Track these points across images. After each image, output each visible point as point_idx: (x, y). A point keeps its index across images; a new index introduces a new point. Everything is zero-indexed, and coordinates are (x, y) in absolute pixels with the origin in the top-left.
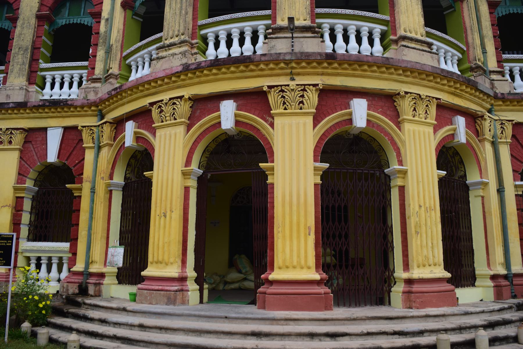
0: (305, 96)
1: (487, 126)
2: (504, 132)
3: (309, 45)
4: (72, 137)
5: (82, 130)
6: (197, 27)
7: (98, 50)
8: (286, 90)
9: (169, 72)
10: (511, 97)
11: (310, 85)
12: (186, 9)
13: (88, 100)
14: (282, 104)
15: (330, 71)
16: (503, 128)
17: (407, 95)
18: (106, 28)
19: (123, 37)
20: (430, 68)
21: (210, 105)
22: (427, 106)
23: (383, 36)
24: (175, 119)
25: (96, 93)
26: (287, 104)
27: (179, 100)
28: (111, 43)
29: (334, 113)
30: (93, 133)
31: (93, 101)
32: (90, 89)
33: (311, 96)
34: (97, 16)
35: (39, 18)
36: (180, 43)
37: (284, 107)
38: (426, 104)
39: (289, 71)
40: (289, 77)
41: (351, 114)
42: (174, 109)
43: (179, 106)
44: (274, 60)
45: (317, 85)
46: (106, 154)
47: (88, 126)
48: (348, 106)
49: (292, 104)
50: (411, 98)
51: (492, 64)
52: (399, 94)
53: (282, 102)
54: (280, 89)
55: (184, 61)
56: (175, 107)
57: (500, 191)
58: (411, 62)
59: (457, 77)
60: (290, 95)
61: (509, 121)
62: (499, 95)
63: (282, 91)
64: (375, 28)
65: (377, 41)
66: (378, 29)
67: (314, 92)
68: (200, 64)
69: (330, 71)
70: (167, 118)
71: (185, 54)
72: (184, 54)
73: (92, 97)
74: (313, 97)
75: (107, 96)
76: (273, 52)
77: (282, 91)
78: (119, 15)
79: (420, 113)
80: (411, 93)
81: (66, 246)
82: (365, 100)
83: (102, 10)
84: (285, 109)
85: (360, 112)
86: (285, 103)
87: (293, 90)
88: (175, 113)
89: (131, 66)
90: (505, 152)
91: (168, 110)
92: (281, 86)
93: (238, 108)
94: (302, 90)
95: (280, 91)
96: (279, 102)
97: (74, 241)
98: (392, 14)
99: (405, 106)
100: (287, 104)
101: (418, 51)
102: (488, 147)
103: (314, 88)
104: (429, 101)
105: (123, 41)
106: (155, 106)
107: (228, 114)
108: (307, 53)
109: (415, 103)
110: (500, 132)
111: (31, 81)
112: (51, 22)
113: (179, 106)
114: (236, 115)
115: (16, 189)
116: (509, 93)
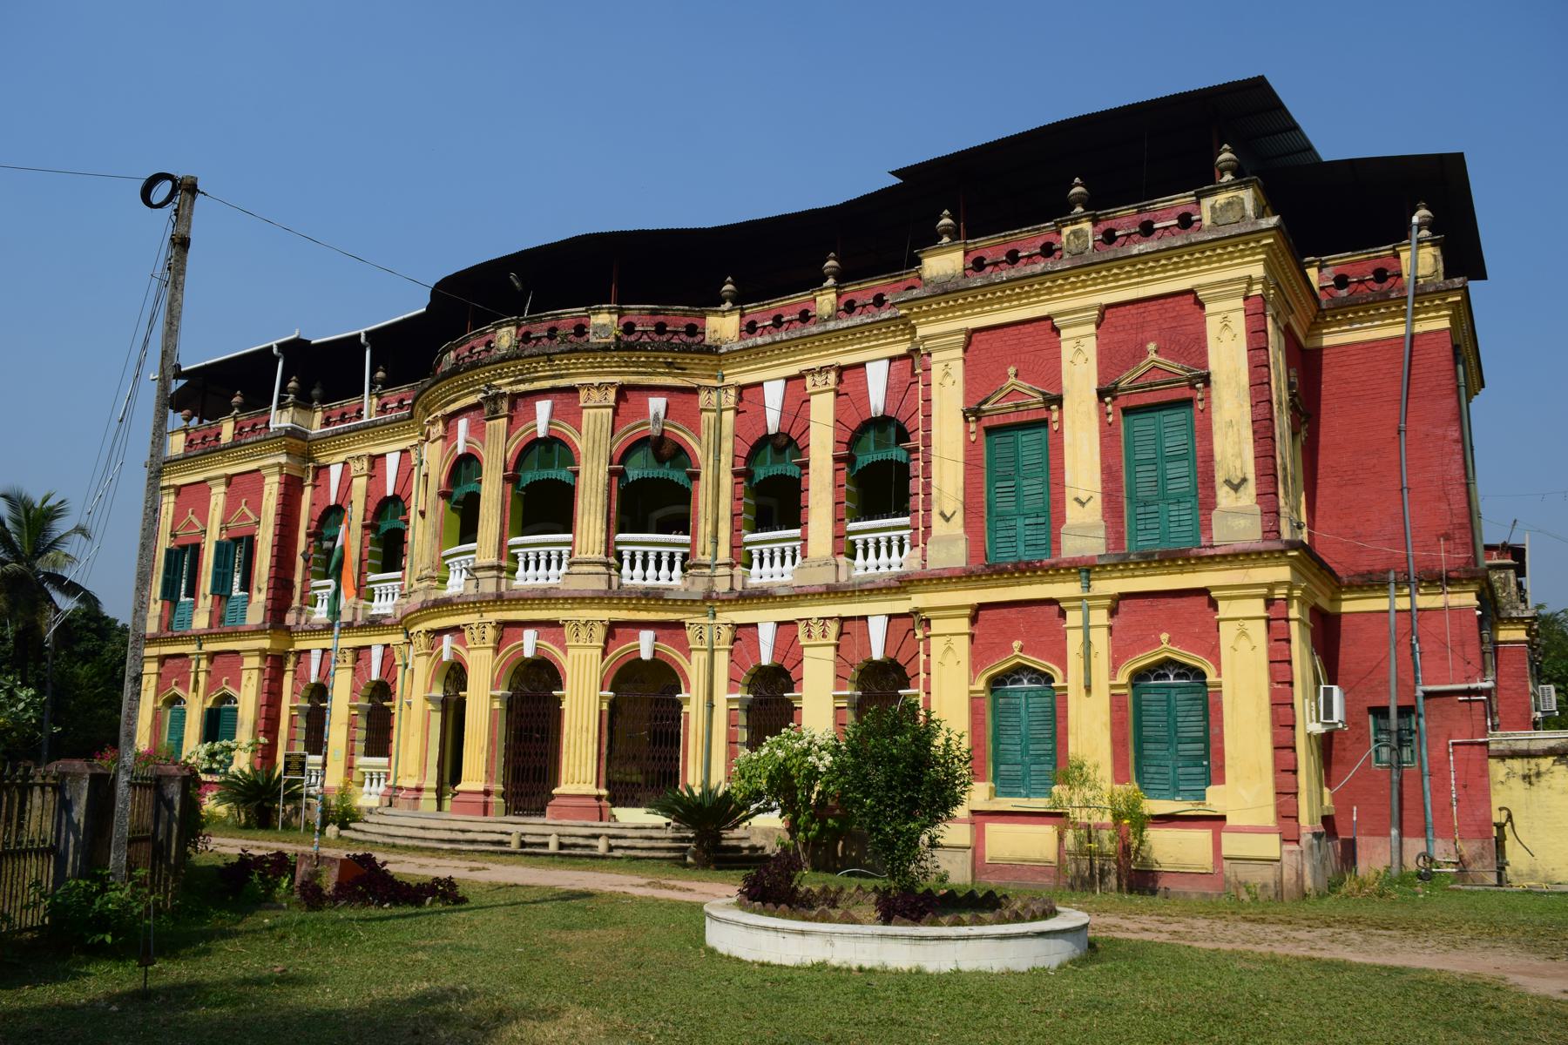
34: (407, 522)
35: (365, 527)
51: (724, 554)
74: (490, 633)
81: (385, 760)
90: (722, 660)
97: (389, 755)
102: (699, 658)
111: (358, 595)
115: (351, 708)
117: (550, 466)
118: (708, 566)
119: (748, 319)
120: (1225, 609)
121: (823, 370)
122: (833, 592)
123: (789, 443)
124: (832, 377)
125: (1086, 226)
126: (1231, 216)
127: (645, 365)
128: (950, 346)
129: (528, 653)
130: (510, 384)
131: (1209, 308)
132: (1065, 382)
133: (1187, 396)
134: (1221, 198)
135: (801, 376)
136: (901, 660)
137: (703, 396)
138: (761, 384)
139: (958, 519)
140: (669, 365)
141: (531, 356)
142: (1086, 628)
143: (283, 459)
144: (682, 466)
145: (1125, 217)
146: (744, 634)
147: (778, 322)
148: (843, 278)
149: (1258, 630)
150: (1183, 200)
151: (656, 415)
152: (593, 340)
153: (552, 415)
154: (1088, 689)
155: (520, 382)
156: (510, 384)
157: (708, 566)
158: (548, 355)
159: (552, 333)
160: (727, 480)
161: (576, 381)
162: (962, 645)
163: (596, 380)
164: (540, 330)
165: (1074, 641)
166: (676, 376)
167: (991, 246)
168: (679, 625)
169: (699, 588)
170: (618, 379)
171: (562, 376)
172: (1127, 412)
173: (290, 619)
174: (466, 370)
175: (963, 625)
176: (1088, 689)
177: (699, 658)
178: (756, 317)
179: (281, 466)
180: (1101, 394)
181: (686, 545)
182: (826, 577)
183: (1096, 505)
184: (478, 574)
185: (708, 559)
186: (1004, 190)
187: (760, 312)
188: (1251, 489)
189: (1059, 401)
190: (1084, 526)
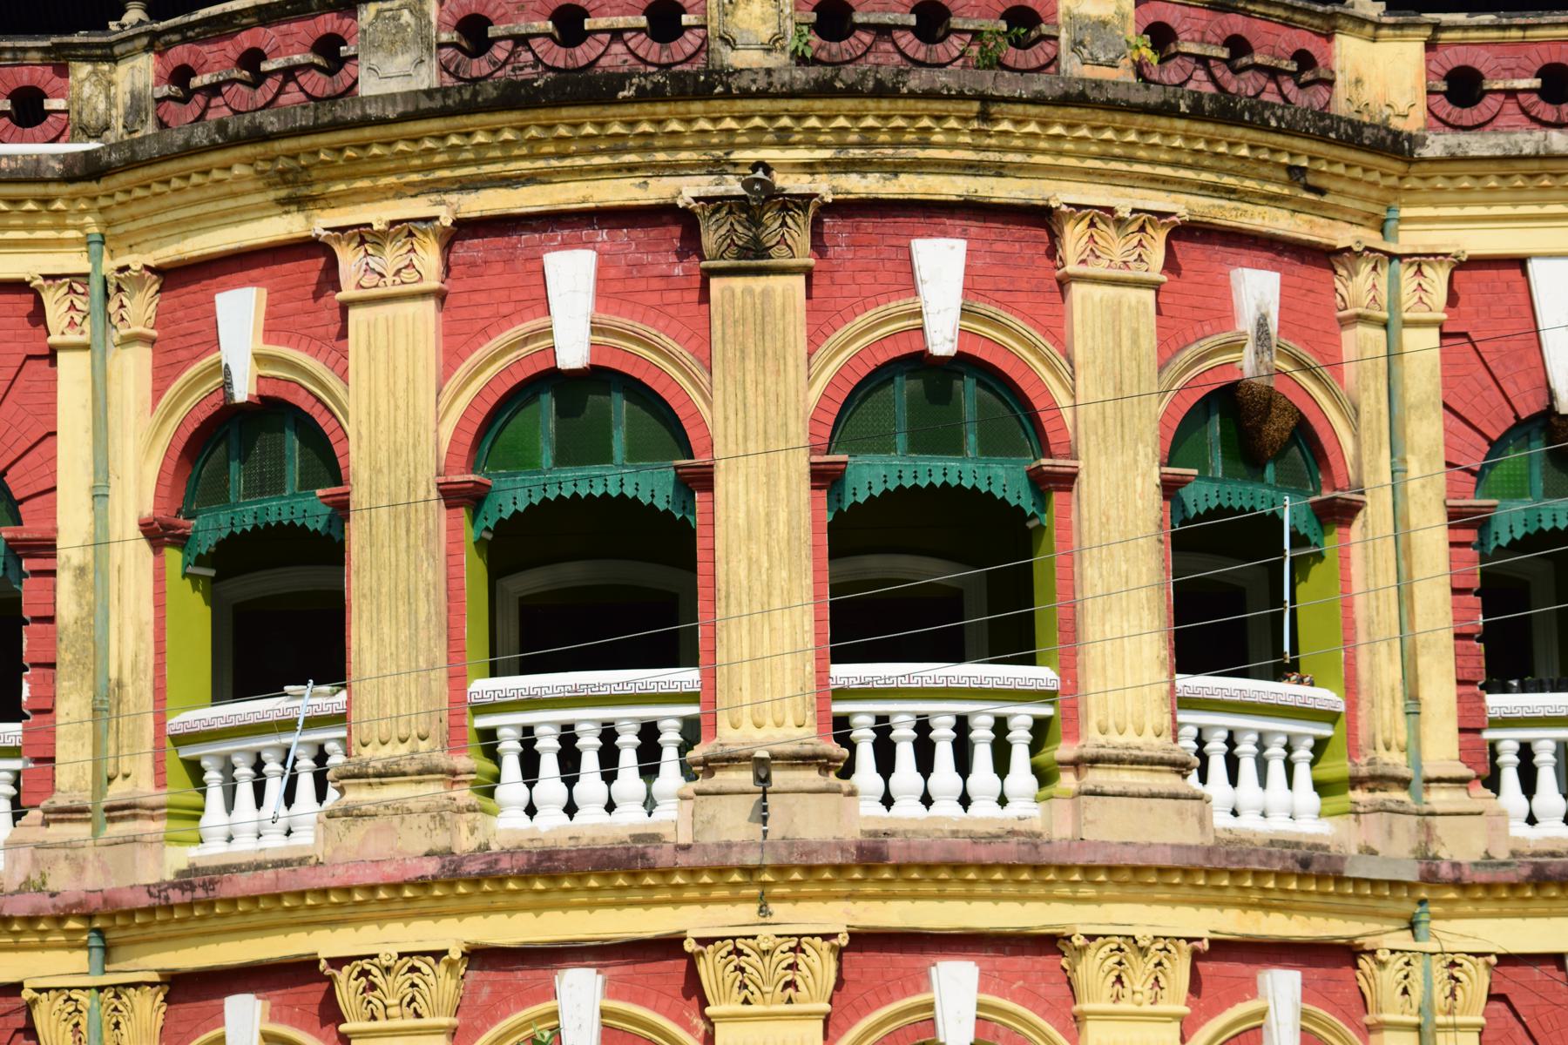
0: (802, 966)
2: (1459, 992)
5: (35, 1001)
6: (461, 706)
7: (59, 692)
8: (747, 950)
9: (391, 872)
10: (1483, 876)
11: (813, 936)
12: (430, 650)
13: (53, 895)
14: (736, 989)
15: (870, 889)
16: (1457, 980)
17: (1093, 945)
18: (80, 605)
19: (160, 651)
20: (1168, 851)
21: (522, 976)
22: (1160, 964)
23: (1040, 729)
24: (418, 1016)
25: (79, 868)
26: (752, 987)
27: (430, 959)
28: (113, 674)
29: (881, 1004)
30: (76, 1010)
31: (73, 900)
32: (52, 853)
33: (816, 966)
36: (420, 773)
37: (742, 998)
38: (1155, 960)
39: (755, 891)
40: (755, 907)
41: (930, 1006)
42: (413, 985)
43: (431, 979)
45: (835, 935)
47: (57, 989)
48: (920, 982)
49: (764, 989)
50: (1107, 948)
51: (1442, 749)
52: (1069, 938)
53: (737, 983)
54: (730, 948)
55: (440, 840)
56: (417, 981)
58: (1105, 844)
59: (1261, 862)
60: (760, 965)
61: (1477, 955)
62: (1445, 871)
63: (739, 953)
64: (1016, 715)
65: (1020, 757)
66: (1021, 718)
67: (825, 954)
68: (497, 861)
69: (870, 889)
70: (390, 1011)
71: (442, 818)
72: (439, 815)
73: (65, 882)
74: (821, 967)
75: (145, 901)
76: (709, 838)
77: (739, 953)
78: (134, 562)
79: (1137, 987)
80: (1105, 936)
82: (972, 963)
83: (55, 530)
84: (746, 1002)
86: (746, 987)
87: (765, 952)
88: (419, 998)
89: (202, 772)
91: (394, 987)
92: (734, 938)
93: (611, 992)
94: (791, 950)
95: (730, 953)
96: (728, 981)
98: (1069, 668)
99: (1092, 970)
100: (752, 987)
101: (1135, 800)
103: (826, 945)
104: (1165, 949)
105: (160, 667)
106: (346, 969)
108: (806, 843)
109: (1120, 963)
110: (1447, 992)
113: (431, 979)
114: (604, 1013)
116: (1488, 861)
117: (953, 446)
118: (1404, 783)
119: (1452, 58)
127: (1243, 167)
130: (810, 167)
137: (1360, 287)
138: (1519, 263)
140: (1295, 174)
141: (930, 95)
144: (1295, 482)
151: (1262, 324)
152: (1073, 67)
153: (973, 286)
155: (860, 167)
156: (810, 167)
157: (1404, 783)
158: (985, 99)
160: (1432, 537)
161: (1060, 194)
163: (1125, 200)
166: (1298, 208)
168: (1347, 954)
170: (1182, 206)
171: (1000, 170)
174: (642, 96)
178: (1481, 60)
181: (1331, 717)
184: (780, 778)
185: (1395, 761)
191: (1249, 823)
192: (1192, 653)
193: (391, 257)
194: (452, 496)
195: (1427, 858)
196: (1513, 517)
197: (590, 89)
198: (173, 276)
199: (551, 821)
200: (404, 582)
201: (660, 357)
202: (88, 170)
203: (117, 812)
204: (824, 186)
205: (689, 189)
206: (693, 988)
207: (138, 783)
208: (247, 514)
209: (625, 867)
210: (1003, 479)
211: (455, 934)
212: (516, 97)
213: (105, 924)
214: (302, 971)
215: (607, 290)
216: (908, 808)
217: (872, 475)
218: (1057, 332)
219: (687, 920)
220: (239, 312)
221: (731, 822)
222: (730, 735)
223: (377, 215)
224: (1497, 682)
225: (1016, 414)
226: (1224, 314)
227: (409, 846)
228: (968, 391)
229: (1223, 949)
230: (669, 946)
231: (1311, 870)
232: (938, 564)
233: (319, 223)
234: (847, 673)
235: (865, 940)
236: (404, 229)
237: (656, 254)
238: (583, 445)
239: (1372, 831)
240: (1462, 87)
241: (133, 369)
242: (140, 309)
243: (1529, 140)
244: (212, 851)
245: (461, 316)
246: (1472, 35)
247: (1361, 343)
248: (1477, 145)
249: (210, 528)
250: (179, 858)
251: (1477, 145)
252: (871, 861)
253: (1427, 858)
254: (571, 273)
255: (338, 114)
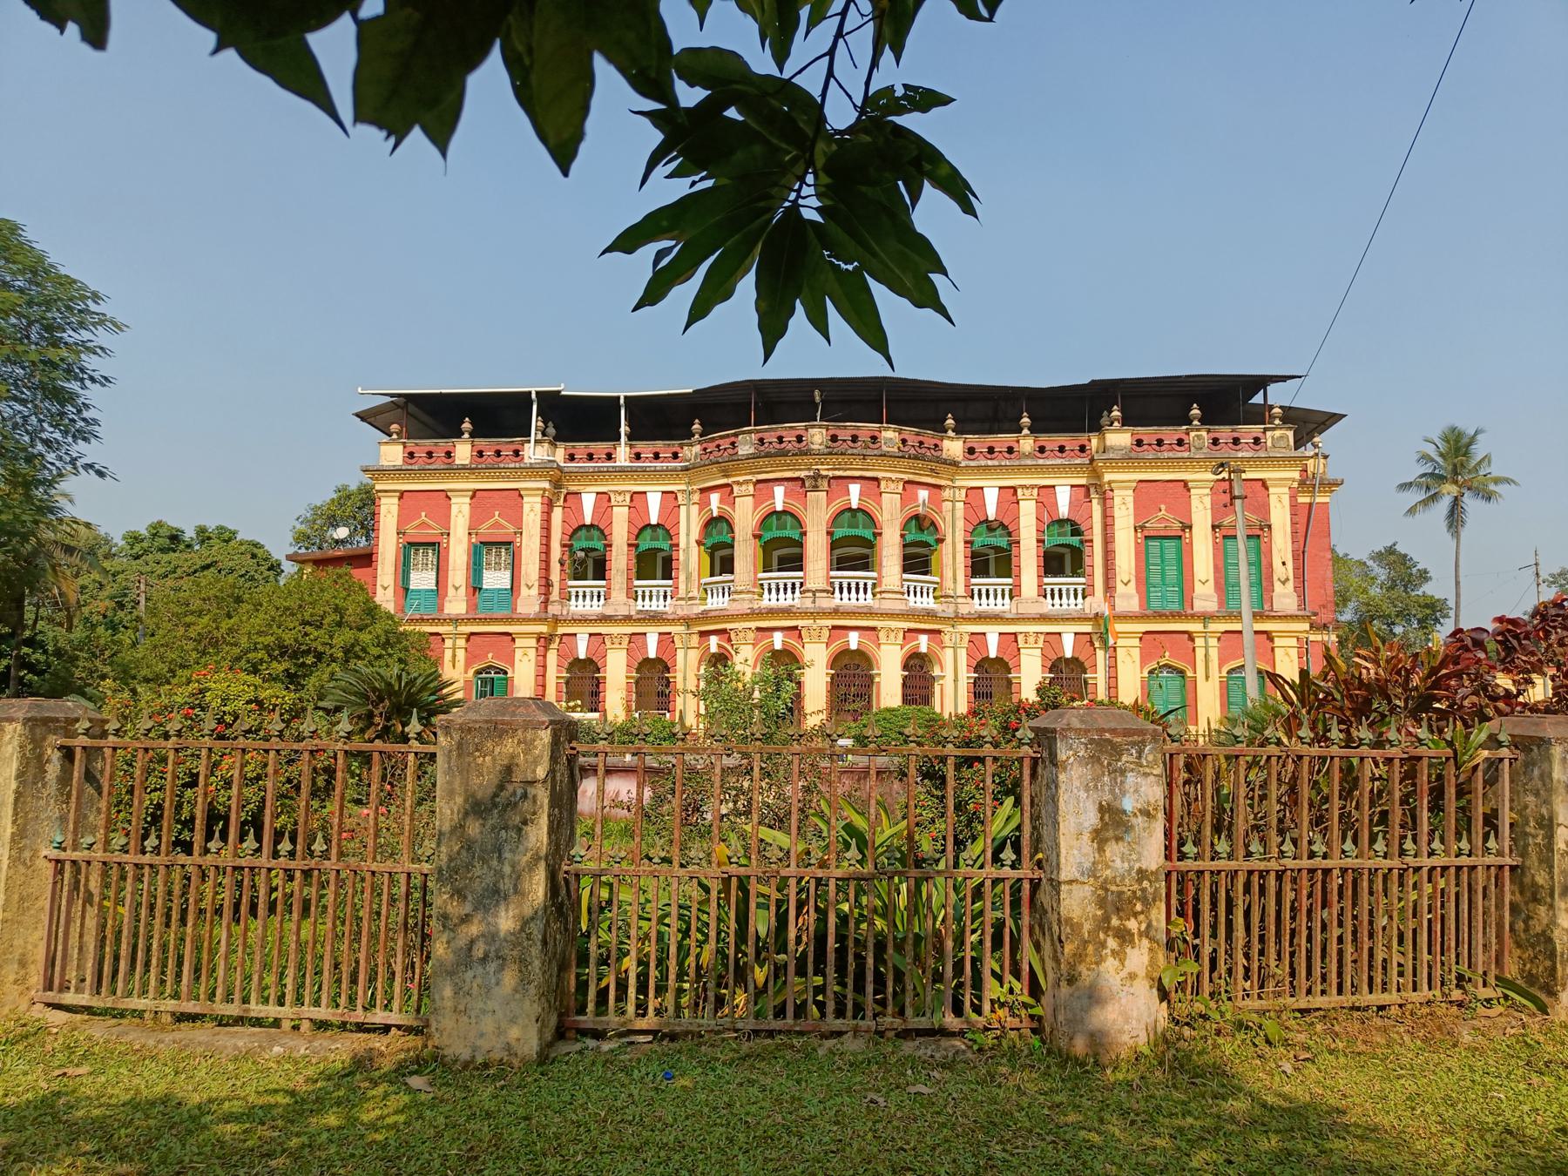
1: (946, 638)
3: (826, 603)
4: (666, 639)
23: (874, 585)
44: (805, 614)
46: (694, 655)
51: (961, 590)
57: (956, 681)
66: (870, 583)
73: (680, 612)
74: (826, 633)
78: (694, 549)
85: (854, 640)
90: (962, 654)
98: (880, 573)
99: (882, 635)
102: (949, 652)
107: (778, 640)
112: (637, 546)
120: (1278, 642)
121: (1033, 487)
122: (1044, 618)
123: (1005, 527)
124: (1035, 491)
125: (1204, 434)
126: (1282, 444)
128: (1126, 488)
129: (854, 646)
131: (1271, 490)
132: (1194, 517)
133: (1260, 533)
134: (1278, 433)
135: (1014, 489)
136: (1082, 659)
137: (947, 494)
139: (1133, 584)
142: (1206, 648)
143: (546, 485)
145: (1225, 432)
146: (978, 639)
147: (991, 450)
148: (1033, 430)
149: (1294, 653)
150: (1256, 429)
152: (885, 448)
153: (861, 494)
154: (1207, 678)
159: (855, 439)
160: (960, 546)
162: (1136, 653)
163: (893, 476)
164: (845, 435)
165: (1200, 653)
167: (1148, 433)
168: (939, 632)
169: (950, 612)
170: (906, 477)
172: (1225, 537)
173: (554, 609)
175: (1136, 642)
176: (1207, 678)
177: (949, 652)
179: (544, 490)
180: (1214, 527)
182: (1034, 610)
183: (1211, 583)
186: (1158, 403)
187: (980, 441)
188: (1290, 585)
189: (1190, 527)
190: (1205, 596)
191: (919, 605)
192: (907, 569)
193: (744, 487)
194: (755, 536)
195: (956, 612)
196: (978, 541)
197: (784, 453)
198: (703, 490)
199: (774, 602)
200: (746, 554)
201: (797, 507)
202: (686, 469)
203: (691, 599)
204: (830, 474)
205: (802, 474)
206: (800, 636)
207: (695, 593)
208: (715, 539)
209: (787, 612)
210: (868, 534)
211: (753, 625)
212: (768, 455)
213: (688, 621)
214: (724, 631)
215: (786, 494)
216: (845, 600)
217: (840, 533)
218: (879, 504)
219: (800, 623)
220: (715, 498)
221: (808, 603)
222: (808, 586)
223: (741, 479)
224: (974, 575)
225: (871, 520)
226: (916, 499)
227: (744, 607)
228: (860, 515)
229: (910, 630)
230: (795, 628)
231: (930, 615)
232: (854, 553)
233: (729, 481)
234: (833, 573)
235: (834, 627)
236: (746, 482)
237: (796, 486)
238: (782, 527)
239: (944, 607)
240: (971, 451)
241: (695, 509)
242: (696, 497)
243: (983, 463)
244: (709, 607)
245: (757, 500)
246: (973, 439)
247: (947, 506)
248: (972, 464)
249: (709, 542)
250: (702, 608)
251: (972, 464)
252: (836, 612)
253: (956, 612)
254: (779, 491)
255: (734, 458)
